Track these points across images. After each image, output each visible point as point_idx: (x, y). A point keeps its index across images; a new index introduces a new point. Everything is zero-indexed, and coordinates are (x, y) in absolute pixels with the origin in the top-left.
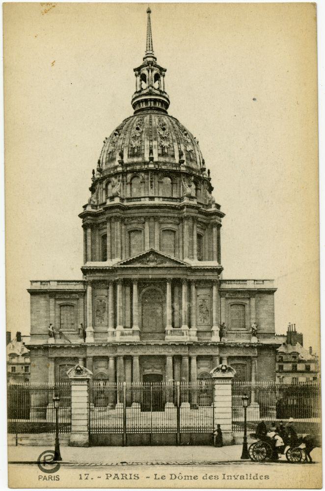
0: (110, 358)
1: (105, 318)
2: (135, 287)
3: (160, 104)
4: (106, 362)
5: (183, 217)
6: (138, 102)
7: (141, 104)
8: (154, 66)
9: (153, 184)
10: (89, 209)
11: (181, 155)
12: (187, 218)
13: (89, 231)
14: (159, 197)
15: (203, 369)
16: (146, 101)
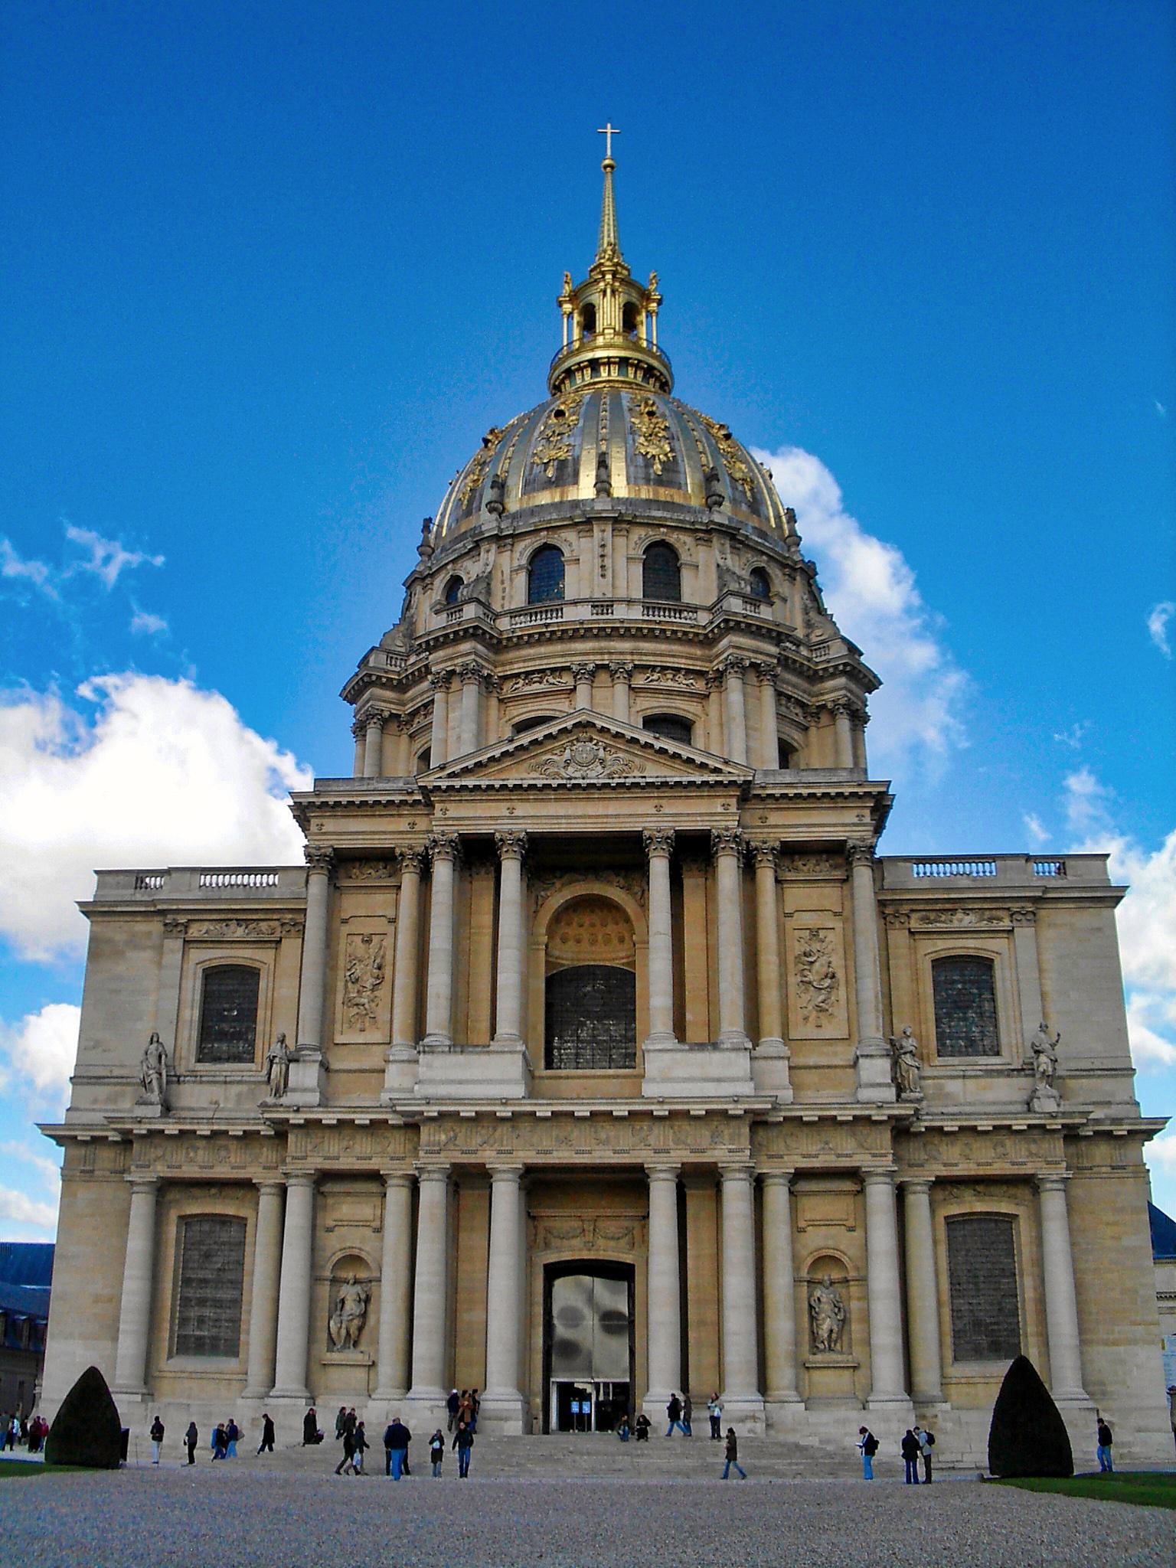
0: (390, 1182)
1: (383, 1015)
2: (511, 870)
3: (640, 374)
4: (377, 1201)
5: (721, 667)
6: (569, 373)
7: (578, 375)
8: (622, 281)
9: (608, 562)
10: (378, 661)
11: (711, 477)
12: (736, 665)
13: (372, 734)
14: (630, 602)
15: (816, 1240)
16: (594, 365)
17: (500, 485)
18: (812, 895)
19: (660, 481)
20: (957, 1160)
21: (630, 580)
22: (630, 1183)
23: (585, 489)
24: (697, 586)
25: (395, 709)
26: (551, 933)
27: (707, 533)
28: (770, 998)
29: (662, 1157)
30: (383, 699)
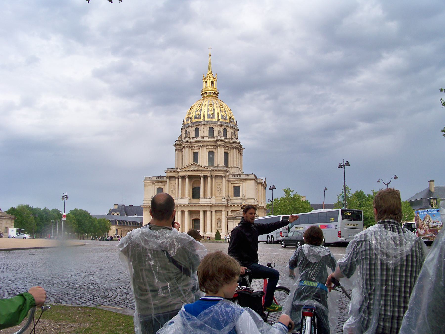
2: (187, 179)
11: (218, 116)
12: (219, 146)
15: (218, 217)
16: (206, 93)
17: (191, 118)
18: (218, 181)
19: (212, 118)
20: (234, 209)
21: (207, 133)
22: (199, 212)
23: (201, 120)
24: (215, 133)
25: (179, 148)
26: (193, 184)
27: (217, 125)
28: (213, 192)
29: (201, 209)
30: (178, 147)
